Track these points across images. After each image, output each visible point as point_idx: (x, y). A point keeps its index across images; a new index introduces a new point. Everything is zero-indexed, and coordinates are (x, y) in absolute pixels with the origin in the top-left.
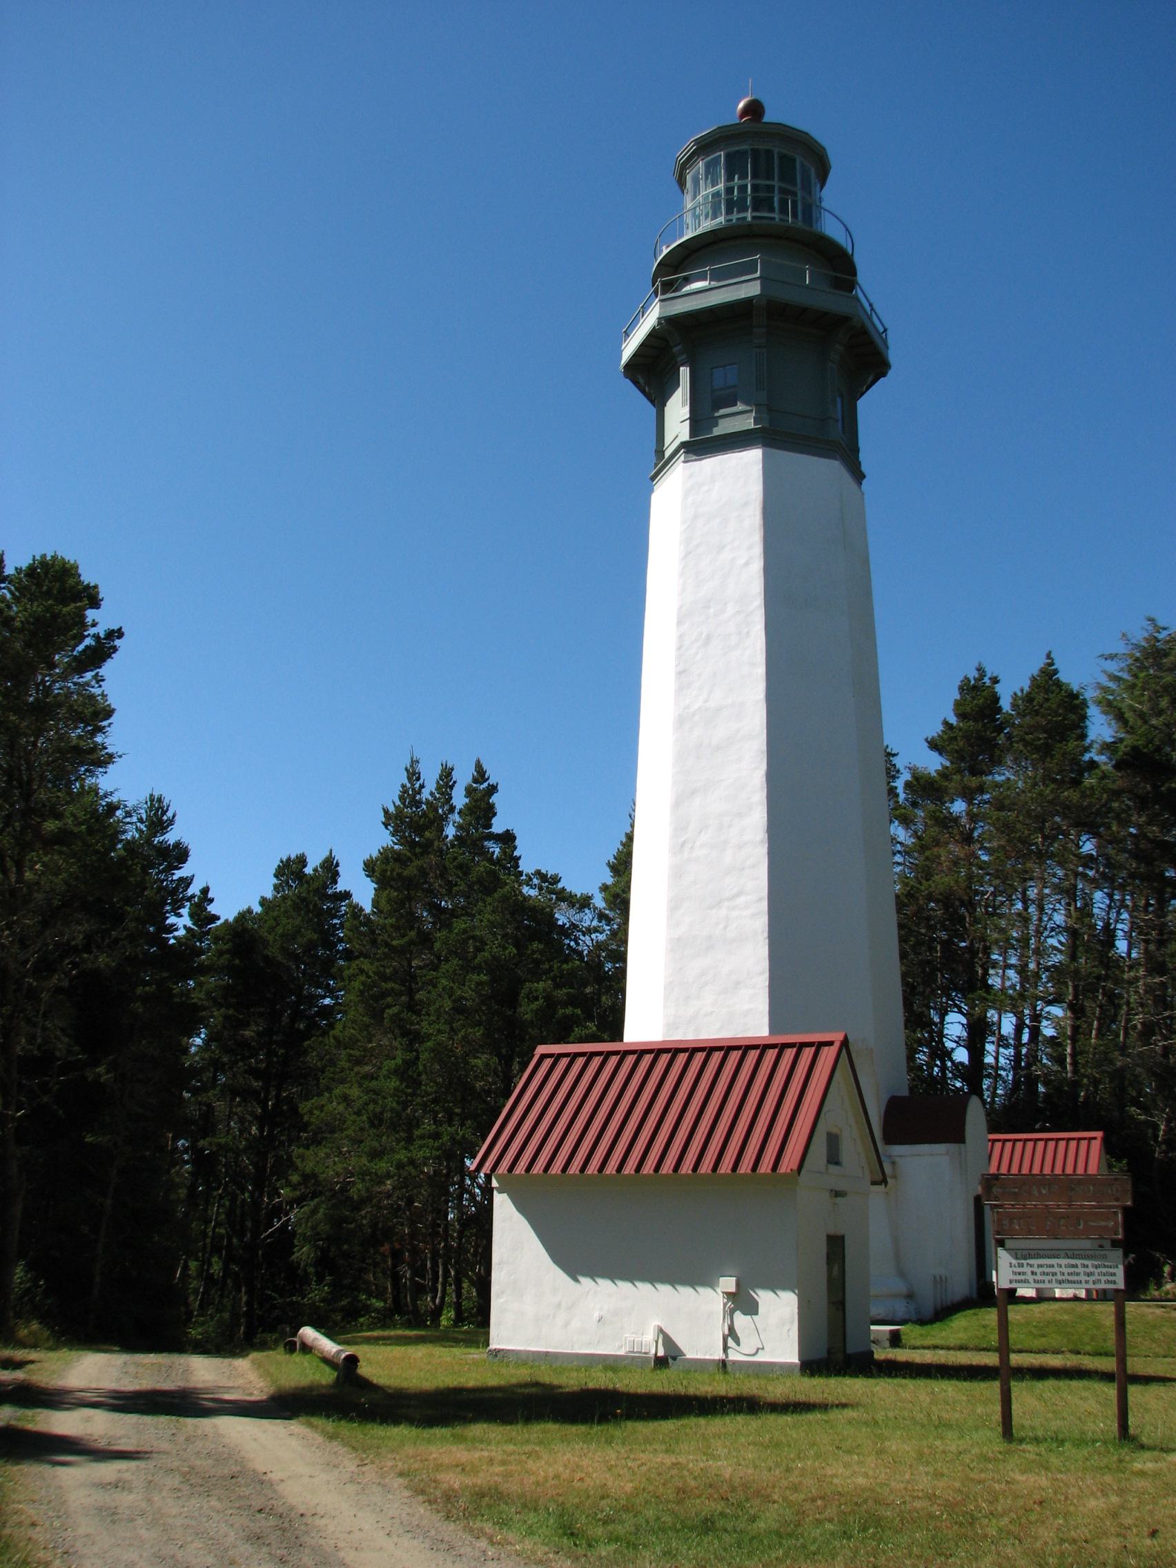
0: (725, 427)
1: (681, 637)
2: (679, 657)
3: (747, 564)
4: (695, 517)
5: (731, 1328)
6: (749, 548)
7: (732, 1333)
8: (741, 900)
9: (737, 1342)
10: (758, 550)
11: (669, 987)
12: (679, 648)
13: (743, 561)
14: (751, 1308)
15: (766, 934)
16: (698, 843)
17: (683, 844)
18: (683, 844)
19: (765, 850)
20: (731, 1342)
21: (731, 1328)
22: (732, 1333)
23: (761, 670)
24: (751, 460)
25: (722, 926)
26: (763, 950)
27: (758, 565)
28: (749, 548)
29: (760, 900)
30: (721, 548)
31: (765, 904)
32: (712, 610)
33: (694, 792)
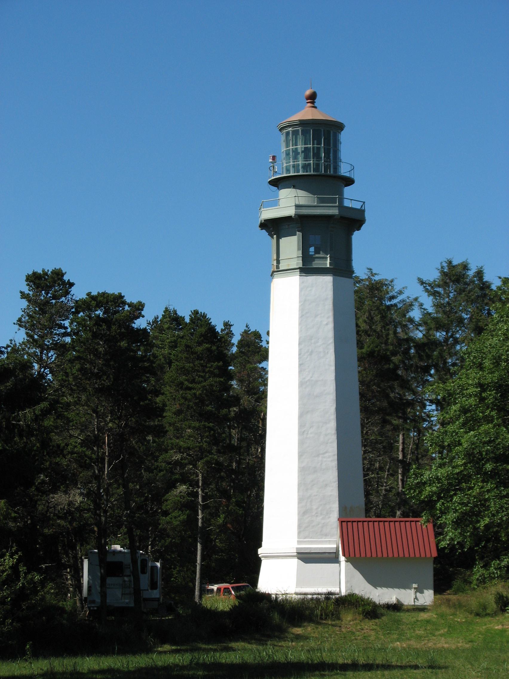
0: (317, 264)
1: (300, 350)
2: (300, 358)
3: (327, 324)
4: (305, 301)
5: (416, 597)
6: (328, 318)
7: (416, 598)
8: (327, 455)
9: (418, 600)
10: (331, 319)
11: (300, 485)
12: (300, 354)
13: (325, 323)
14: (422, 592)
15: (337, 468)
16: (310, 432)
17: (304, 432)
18: (304, 432)
19: (336, 437)
20: (416, 600)
21: (416, 597)
22: (416, 598)
23: (333, 368)
24: (327, 280)
25: (320, 464)
26: (336, 474)
27: (331, 326)
28: (328, 318)
29: (334, 455)
30: (316, 316)
31: (336, 457)
32: (313, 341)
33: (308, 412)
